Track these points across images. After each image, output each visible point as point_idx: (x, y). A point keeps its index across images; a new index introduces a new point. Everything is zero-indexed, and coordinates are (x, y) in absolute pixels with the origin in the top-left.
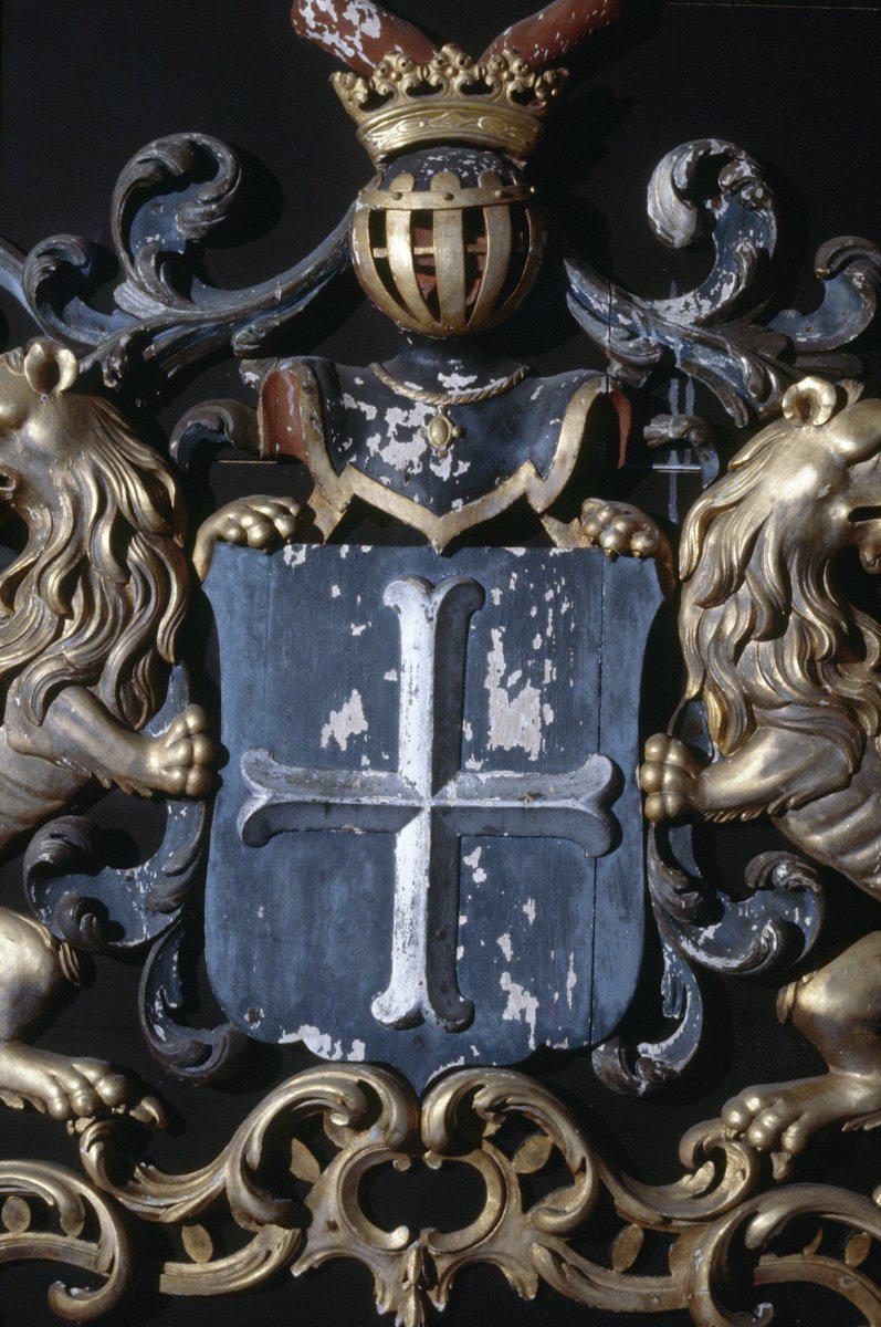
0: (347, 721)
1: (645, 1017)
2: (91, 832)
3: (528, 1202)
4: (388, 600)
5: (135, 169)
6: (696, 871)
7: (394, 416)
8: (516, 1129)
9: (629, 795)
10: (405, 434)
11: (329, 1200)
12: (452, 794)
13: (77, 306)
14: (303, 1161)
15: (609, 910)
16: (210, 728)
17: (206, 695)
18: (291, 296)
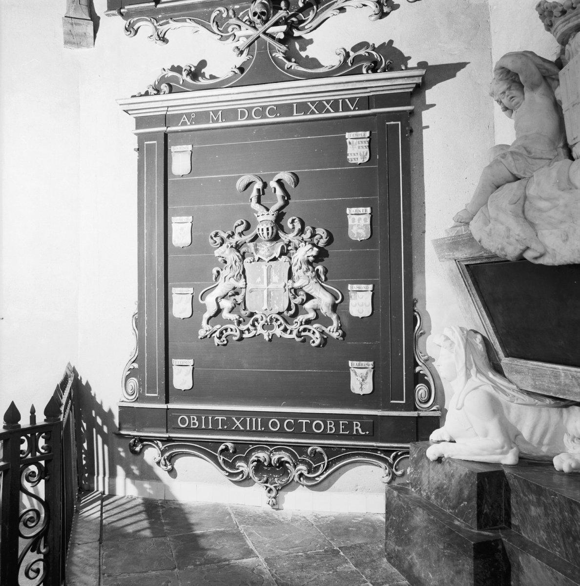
0: (259, 280)
1: (289, 309)
2: (235, 292)
3: (279, 327)
4: (262, 267)
5: (236, 224)
6: (294, 294)
7: (262, 248)
8: (277, 320)
9: (287, 286)
10: (263, 250)
11: (259, 327)
12: (269, 287)
13: (231, 238)
14: (256, 324)
15: (285, 298)
16: (246, 281)
17: (245, 277)
18: (251, 237)
